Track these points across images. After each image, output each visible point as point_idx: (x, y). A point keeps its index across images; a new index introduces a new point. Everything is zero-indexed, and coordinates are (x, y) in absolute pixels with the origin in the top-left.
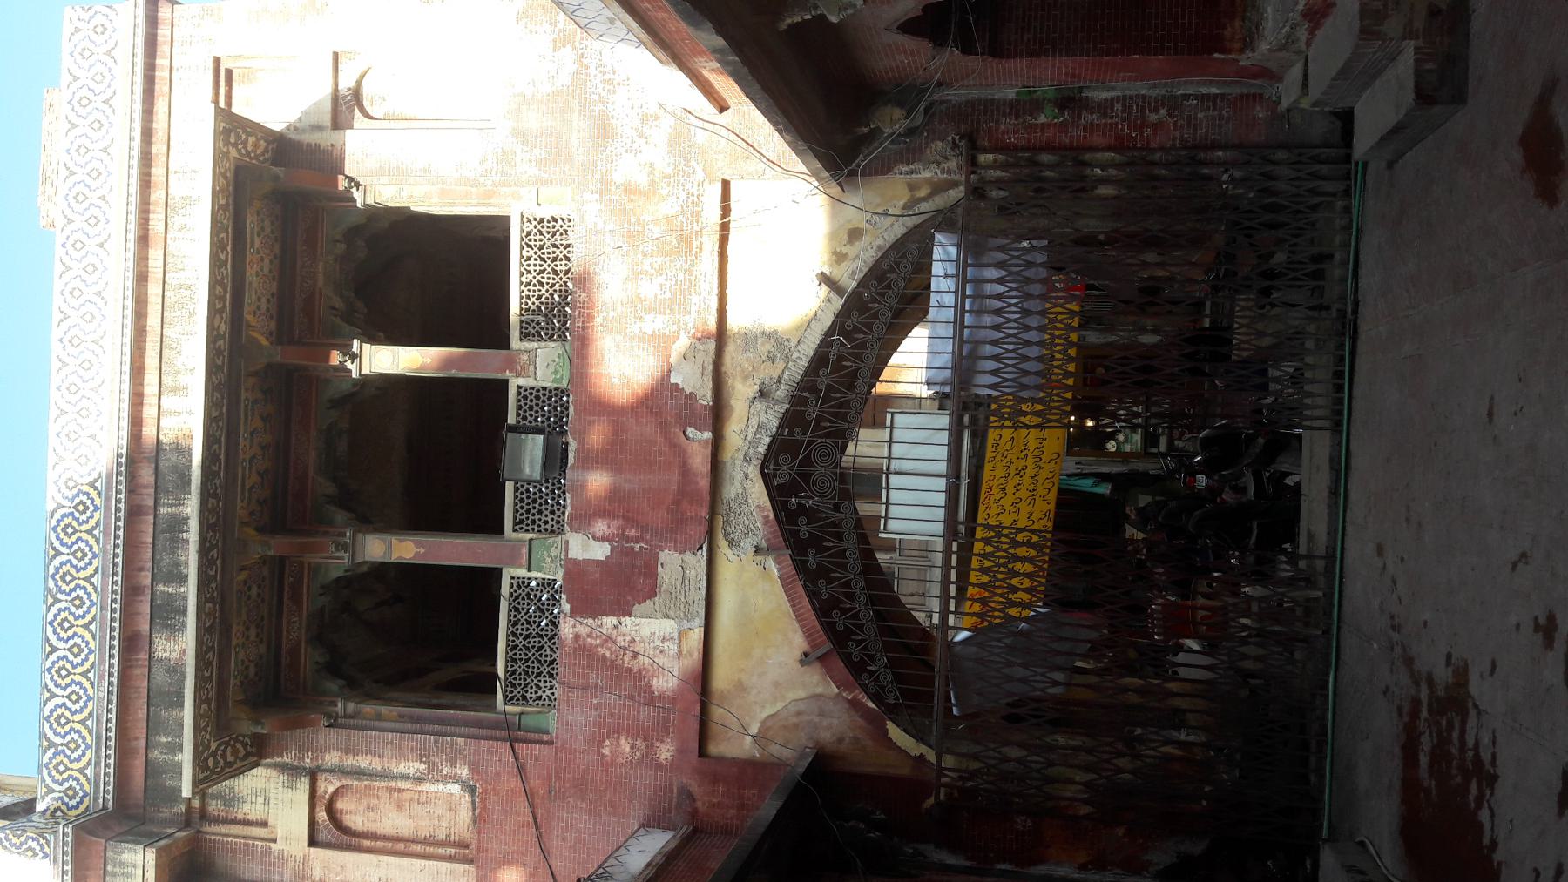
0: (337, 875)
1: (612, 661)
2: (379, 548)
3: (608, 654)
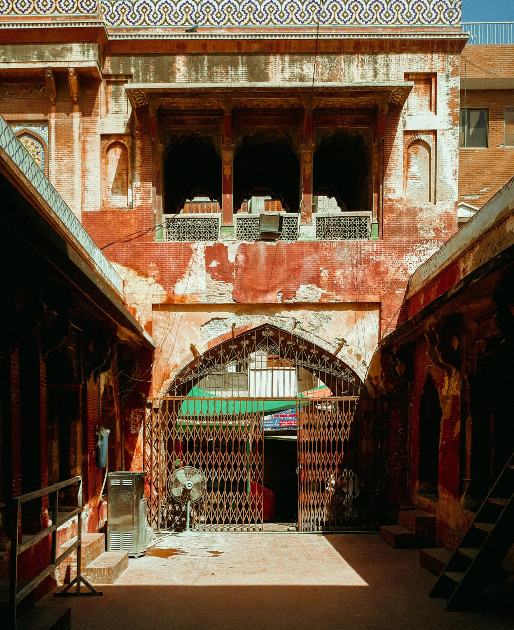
0: (90, 148)
1: (187, 265)
2: (227, 156)
3: (190, 263)
